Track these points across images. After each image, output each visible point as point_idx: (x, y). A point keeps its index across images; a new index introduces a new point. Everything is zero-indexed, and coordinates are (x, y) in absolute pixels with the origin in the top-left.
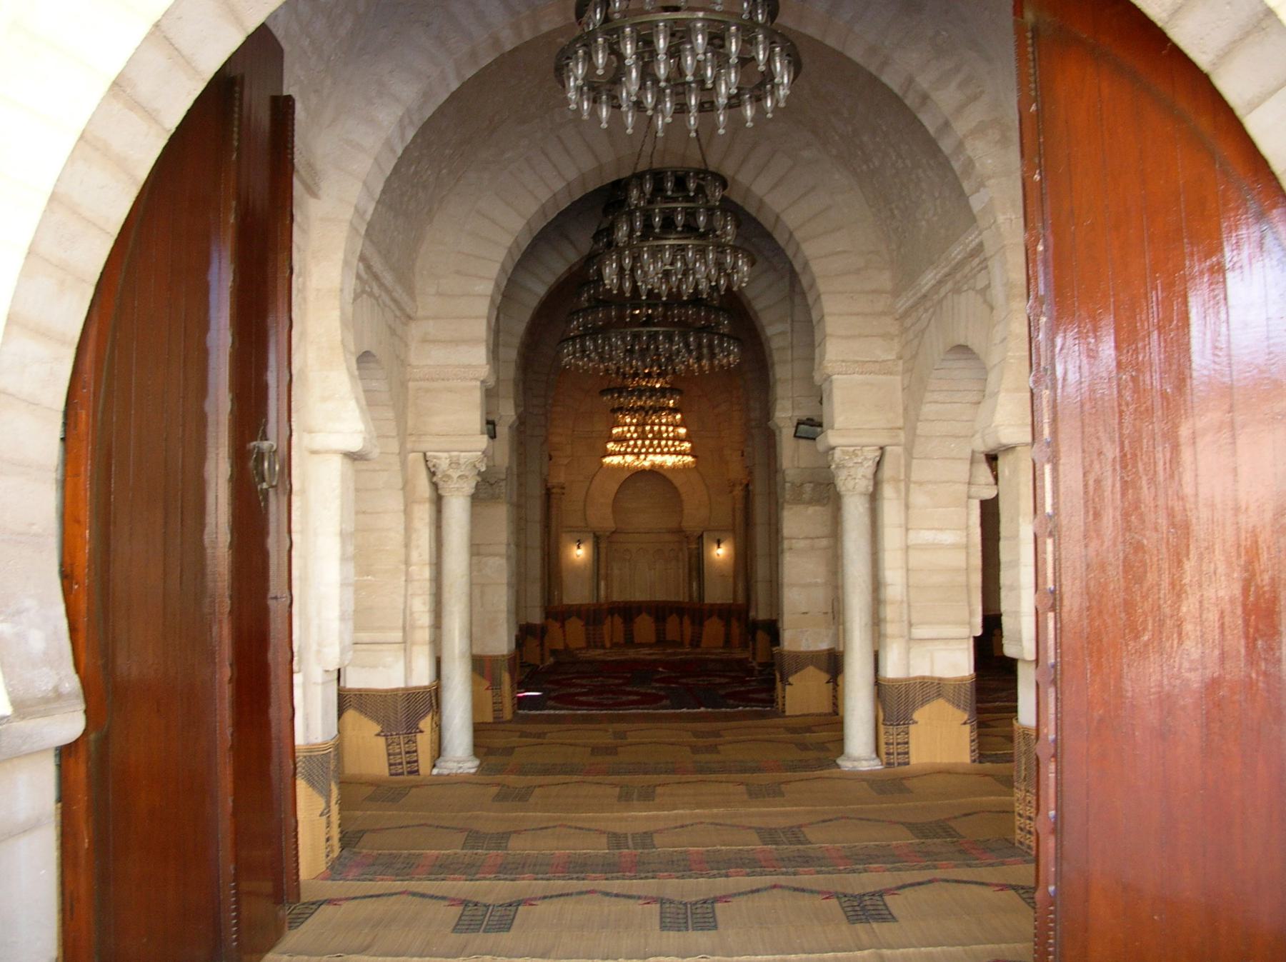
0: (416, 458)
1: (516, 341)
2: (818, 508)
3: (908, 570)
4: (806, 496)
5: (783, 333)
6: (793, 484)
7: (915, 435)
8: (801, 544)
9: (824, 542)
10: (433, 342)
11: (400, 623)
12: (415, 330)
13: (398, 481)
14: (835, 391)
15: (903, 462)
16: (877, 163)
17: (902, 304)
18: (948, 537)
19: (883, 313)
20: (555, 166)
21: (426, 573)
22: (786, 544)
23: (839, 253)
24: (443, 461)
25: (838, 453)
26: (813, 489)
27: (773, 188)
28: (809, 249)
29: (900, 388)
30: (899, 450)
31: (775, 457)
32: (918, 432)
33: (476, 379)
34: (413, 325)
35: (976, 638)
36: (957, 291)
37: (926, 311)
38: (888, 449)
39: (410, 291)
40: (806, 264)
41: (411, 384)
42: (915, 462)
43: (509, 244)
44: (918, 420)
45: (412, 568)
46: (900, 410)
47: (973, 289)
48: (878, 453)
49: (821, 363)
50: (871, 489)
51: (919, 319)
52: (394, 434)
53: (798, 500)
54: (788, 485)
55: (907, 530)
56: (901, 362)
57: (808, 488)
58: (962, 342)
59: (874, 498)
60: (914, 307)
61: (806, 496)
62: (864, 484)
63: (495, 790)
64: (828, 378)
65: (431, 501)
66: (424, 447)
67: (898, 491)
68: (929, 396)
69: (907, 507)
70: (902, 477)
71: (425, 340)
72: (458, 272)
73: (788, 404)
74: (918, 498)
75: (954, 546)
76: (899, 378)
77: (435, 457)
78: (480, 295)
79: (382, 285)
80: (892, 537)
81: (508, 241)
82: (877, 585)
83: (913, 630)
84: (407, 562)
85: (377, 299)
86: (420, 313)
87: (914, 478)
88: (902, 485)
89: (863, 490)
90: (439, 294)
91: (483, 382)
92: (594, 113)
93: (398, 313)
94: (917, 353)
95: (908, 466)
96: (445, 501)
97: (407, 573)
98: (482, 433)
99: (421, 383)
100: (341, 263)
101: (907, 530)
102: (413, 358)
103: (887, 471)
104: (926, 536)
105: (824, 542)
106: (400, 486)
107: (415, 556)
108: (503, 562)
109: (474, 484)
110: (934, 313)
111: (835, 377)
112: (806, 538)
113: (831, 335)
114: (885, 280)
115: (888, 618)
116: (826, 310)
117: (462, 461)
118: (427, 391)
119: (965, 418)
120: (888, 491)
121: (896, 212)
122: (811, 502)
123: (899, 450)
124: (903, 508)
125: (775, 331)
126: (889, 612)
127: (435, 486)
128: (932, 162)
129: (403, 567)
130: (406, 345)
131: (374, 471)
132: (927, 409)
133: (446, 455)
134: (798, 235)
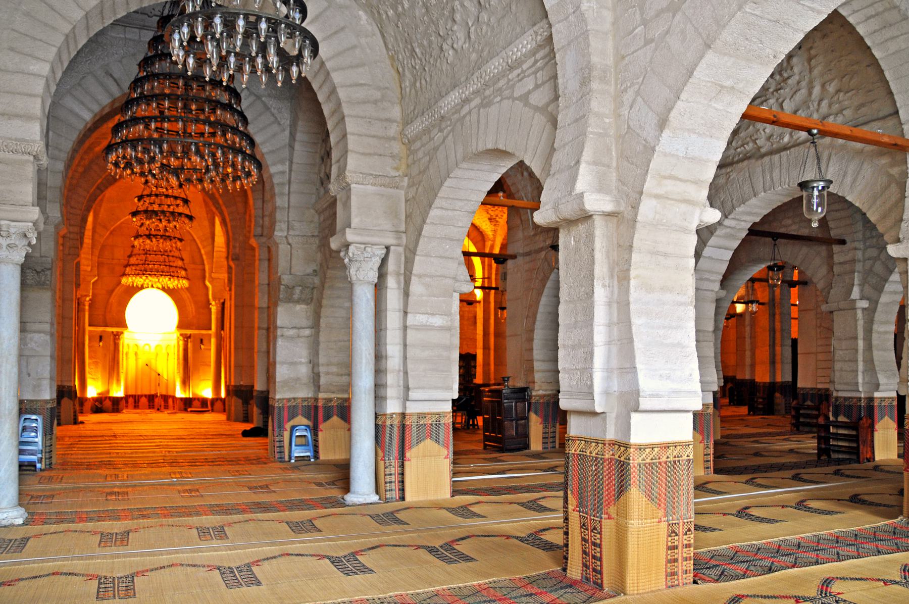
2: (303, 306)
3: (405, 345)
4: (296, 297)
5: (283, 172)
6: (287, 287)
8: (292, 332)
9: (307, 332)
14: (353, 197)
15: (403, 259)
18: (438, 321)
19: (394, 139)
22: (279, 332)
23: (361, 85)
26: (301, 292)
30: (401, 249)
36: (486, 104)
37: (441, 130)
38: (392, 248)
46: (403, 218)
47: (508, 98)
48: (384, 251)
50: (376, 280)
51: (431, 139)
53: (289, 300)
55: (406, 313)
56: (406, 179)
57: (298, 290)
58: (490, 146)
59: (379, 287)
60: (427, 131)
61: (296, 297)
62: (373, 276)
64: (347, 189)
67: (398, 283)
68: (437, 202)
69: (406, 294)
70: (402, 271)
73: (284, 226)
74: (416, 287)
75: (441, 328)
76: (403, 192)
80: (393, 320)
82: (379, 357)
87: (414, 272)
88: (402, 278)
94: (428, 167)
101: (406, 313)
103: (391, 266)
105: (307, 332)
110: (452, 130)
111: (353, 186)
112: (295, 328)
114: (396, 112)
115: (389, 383)
117: (12, 230)
119: (460, 224)
120: (391, 282)
121: (417, 50)
122: (298, 302)
126: (392, 380)
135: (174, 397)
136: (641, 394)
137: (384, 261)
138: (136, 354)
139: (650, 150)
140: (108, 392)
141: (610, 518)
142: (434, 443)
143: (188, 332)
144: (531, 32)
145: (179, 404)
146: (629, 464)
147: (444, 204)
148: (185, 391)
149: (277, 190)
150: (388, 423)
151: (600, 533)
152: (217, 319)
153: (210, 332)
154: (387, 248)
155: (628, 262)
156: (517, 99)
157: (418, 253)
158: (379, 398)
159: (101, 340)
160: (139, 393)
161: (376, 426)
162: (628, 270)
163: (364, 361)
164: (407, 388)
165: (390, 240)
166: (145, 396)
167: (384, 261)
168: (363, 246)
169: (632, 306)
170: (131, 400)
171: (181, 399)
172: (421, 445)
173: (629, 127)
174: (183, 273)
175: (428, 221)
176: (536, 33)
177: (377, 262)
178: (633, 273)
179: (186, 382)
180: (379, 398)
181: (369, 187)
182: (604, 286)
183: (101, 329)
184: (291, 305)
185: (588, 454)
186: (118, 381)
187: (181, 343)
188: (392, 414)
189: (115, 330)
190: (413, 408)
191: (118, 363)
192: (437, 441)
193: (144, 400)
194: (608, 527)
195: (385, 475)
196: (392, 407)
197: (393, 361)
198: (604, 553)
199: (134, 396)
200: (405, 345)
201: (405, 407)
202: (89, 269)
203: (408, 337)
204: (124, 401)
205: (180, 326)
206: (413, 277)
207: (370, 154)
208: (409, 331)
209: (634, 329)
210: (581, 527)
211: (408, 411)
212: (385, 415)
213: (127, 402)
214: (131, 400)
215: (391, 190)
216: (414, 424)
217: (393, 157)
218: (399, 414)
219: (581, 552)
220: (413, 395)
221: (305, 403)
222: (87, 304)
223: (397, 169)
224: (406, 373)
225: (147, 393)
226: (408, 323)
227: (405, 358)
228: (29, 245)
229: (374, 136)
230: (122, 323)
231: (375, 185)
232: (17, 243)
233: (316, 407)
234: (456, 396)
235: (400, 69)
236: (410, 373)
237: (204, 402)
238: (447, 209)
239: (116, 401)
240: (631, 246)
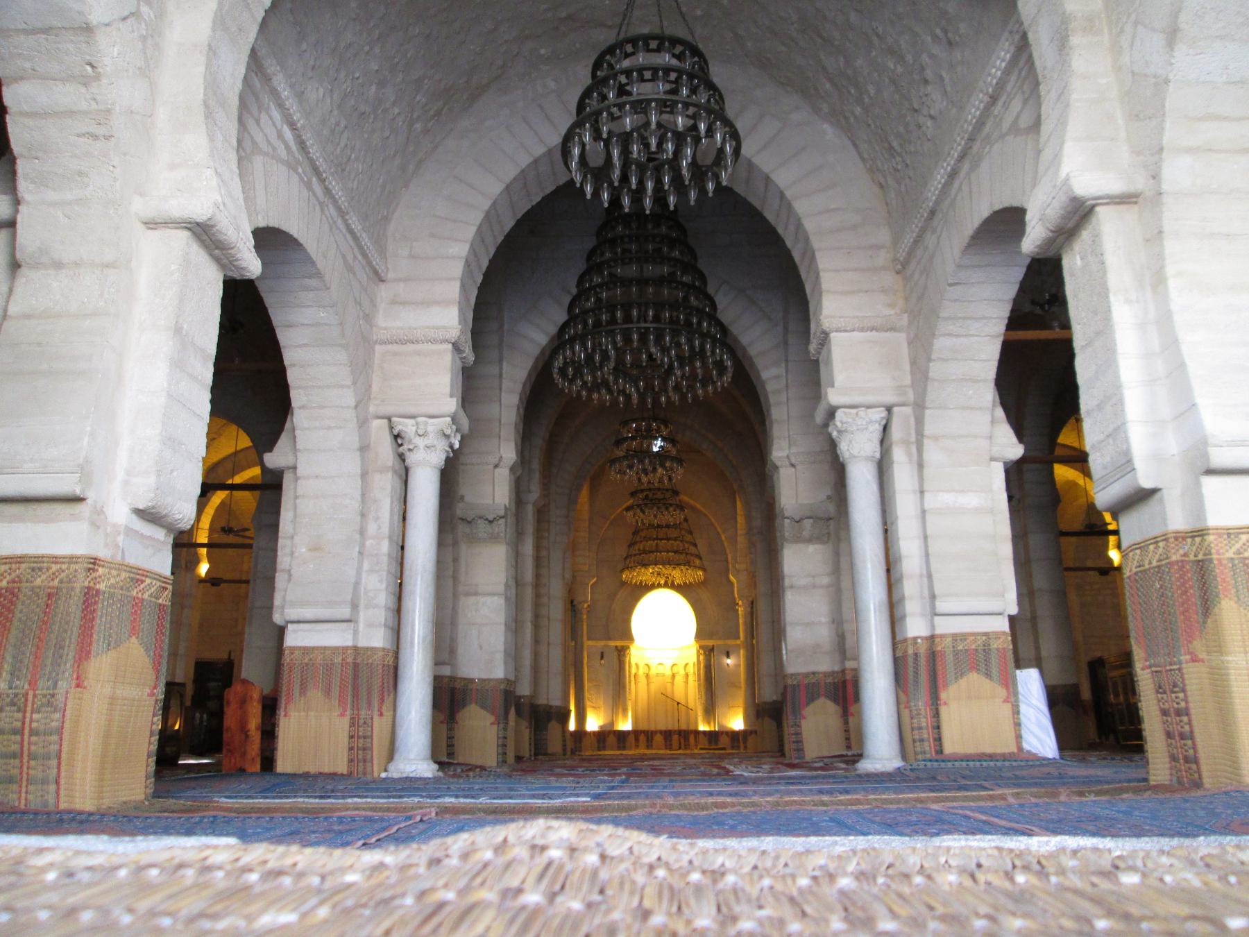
0: (378, 426)
1: (519, 387)
2: (819, 547)
3: (926, 538)
4: (806, 534)
5: (777, 377)
7: (927, 378)
9: (826, 580)
10: (404, 303)
11: (349, 598)
12: (384, 292)
13: (354, 441)
15: (912, 420)
16: (872, 92)
17: (908, 239)
18: (971, 501)
19: (884, 268)
20: (536, 134)
21: (385, 547)
22: (787, 582)
24: (407, 427)
25: (839, 414)
27: (765, 147)
28: (801, 207)
29: (905, 345)
30: (908, 410)
31: (779, 612)
32: (931, 375)
33: (446, 341)
34: (382, 286)
35: (1012, 619)
38: (896, 409)
39: (382, 252)
40: (799, 225)
41: (378, 348)
42: (928, 412)
43: (486, 207)
44: (930, 360)
45: (368, 543)
48: (884, 414)
49: (818, 322)
50: (878, 455)
51: (926, 248)
52: (349, 383)
53: (798, 539)
54: (787, 521)
57: (808, 524)
59: (883, 468)
61: (806, 534)
63: (247, 534)
65: (395, 472)
66: (389, 410)
67: (909, 455)
68: (943, 327)
70: (913, 439)
71: (394, 302)
72: (433, 235)
73: (785, 444)
74: (933, 454)
76: (902, 337)
77: (400, 424)
78: (453, 257)
79: (327, 191)
80: (905, 506)
81: (487, 204)
83: (938, 604)
84: (362, 532)
85: (321, 204)
86: (391, 275)
87: (927, 432)
88: (914, 449)
89: (869, 453)
90: (413, 257)
91: (456, 347)
92: (596, 193)
93: (360, 257)
95: (920, 421)
96: (411, 473)
97: (362, 545)
98: (451, 396)
99: (390, 347)
100: (212, 15)
101: (922, 492)
102: (381, 321)
103: (896, 433)
104: (946, 499)
106: (357, 445)
107: (372, 528)
108: (502, 601)
109: (443, 457)
111: (832, 335)
113: (828, 291)
114: (883, 235)
116: (821, 266)
117: (430, 429)
118: (396, 354)
119: (984, 357)
120: (899, 456)
121: (895, 144)
122: (810, 540)
123: (908, 410)
124: (916, 466)
125: (773, 377)
126: (911, 589)
127: (402, 457)
128: (938, 31)
129: (358, 536)
130: (374, 305)
131: (329, 428)
132: (941, 344)
133: (412, 421)
134: (788, 194)
135: (697, 733)
136: (1211, 441)
137: (886, 428)
138: (647, 676)
139: (1163, 82)
140: (612, 724)
141: (1195, 659)
142: (983, 678)
143: (710, 643)
144: (1006, 34)
145: (703, 741)
146: (1211, 561)
147: (951, 328)
148: (709, 723)
149: (772, 399)
150: (911, 651)
151: (1184, 691)
152: (745, 623)
153: (738, 642)
154: (889, 409)
155: (1160, 257)
156: (1006, 134)
157: (928, 405)
158: (895, 618)
159: (602, 657)
160: (653, 728)
161: (896, 660)
162: (1162, 267)
163: (869, 566)
164: (933, 597)
165: (890, 399)
166: (661, 732)
167: (886, 428)
168: (854, 411)
169: (1176, 318)
170: (642, 738)
171: (704, 732)
172: (963, 682)
173: (1133, 74)
174: (697, 562)
175: (933, 357)
176: (1011, 32)
177: (876, 429)
178: (1170, 270)
179: (710, 710)
180: (895, 618)
181: (856, 334)
182: (1128, 301)
183: (602, 643)
184: (801, 546)
185: (1147, 566)
186: (625, 711)
187: (702, 657)
188: (915, 639)
189: (619, 643)
190: (945, 627)
191: (624, 687)
192: (988, 675)
193: (659, 739)
194: (1194, 677)
195: (913, 729)
196: (915, 627)
197: (911, 563)
198: (1194, 723)
199: (646, 733)
200: (926, 538)
201: (933, 627)
202: (586, 568)
203: (928, 524)
204: (632, 737)
205: (699, 636)
206: (926, 441)
207: (852, 292)
208: (928, 517)
209: (1185, 349)
210: (1158, 692)
211: (938, 631)
212: (905, 640)
213: (637, 740)
214: (642, 738)
215: (888, 334)
216: (949, 651)
217: (884, 291)
218: (926, 638)
219: (1163, 737)
220: (941, 606)
221: (830, 680)
222: (585, 612)
223: (892, 306)
224: (930, 576)
225: (664, 728)
226: (927, 506)
227: (927, 555)
228: (451, 446)
229: (856, 270)
230: (627, 635)
231: (862, 330)
232: (435, 442)
233: (844, 682)
234: (1014, 610)
235: (882, 180)
236: (935, 576)
237: (734, 735)
238: (958, 336)
239: (622, 735)
240: (1160, 232)
